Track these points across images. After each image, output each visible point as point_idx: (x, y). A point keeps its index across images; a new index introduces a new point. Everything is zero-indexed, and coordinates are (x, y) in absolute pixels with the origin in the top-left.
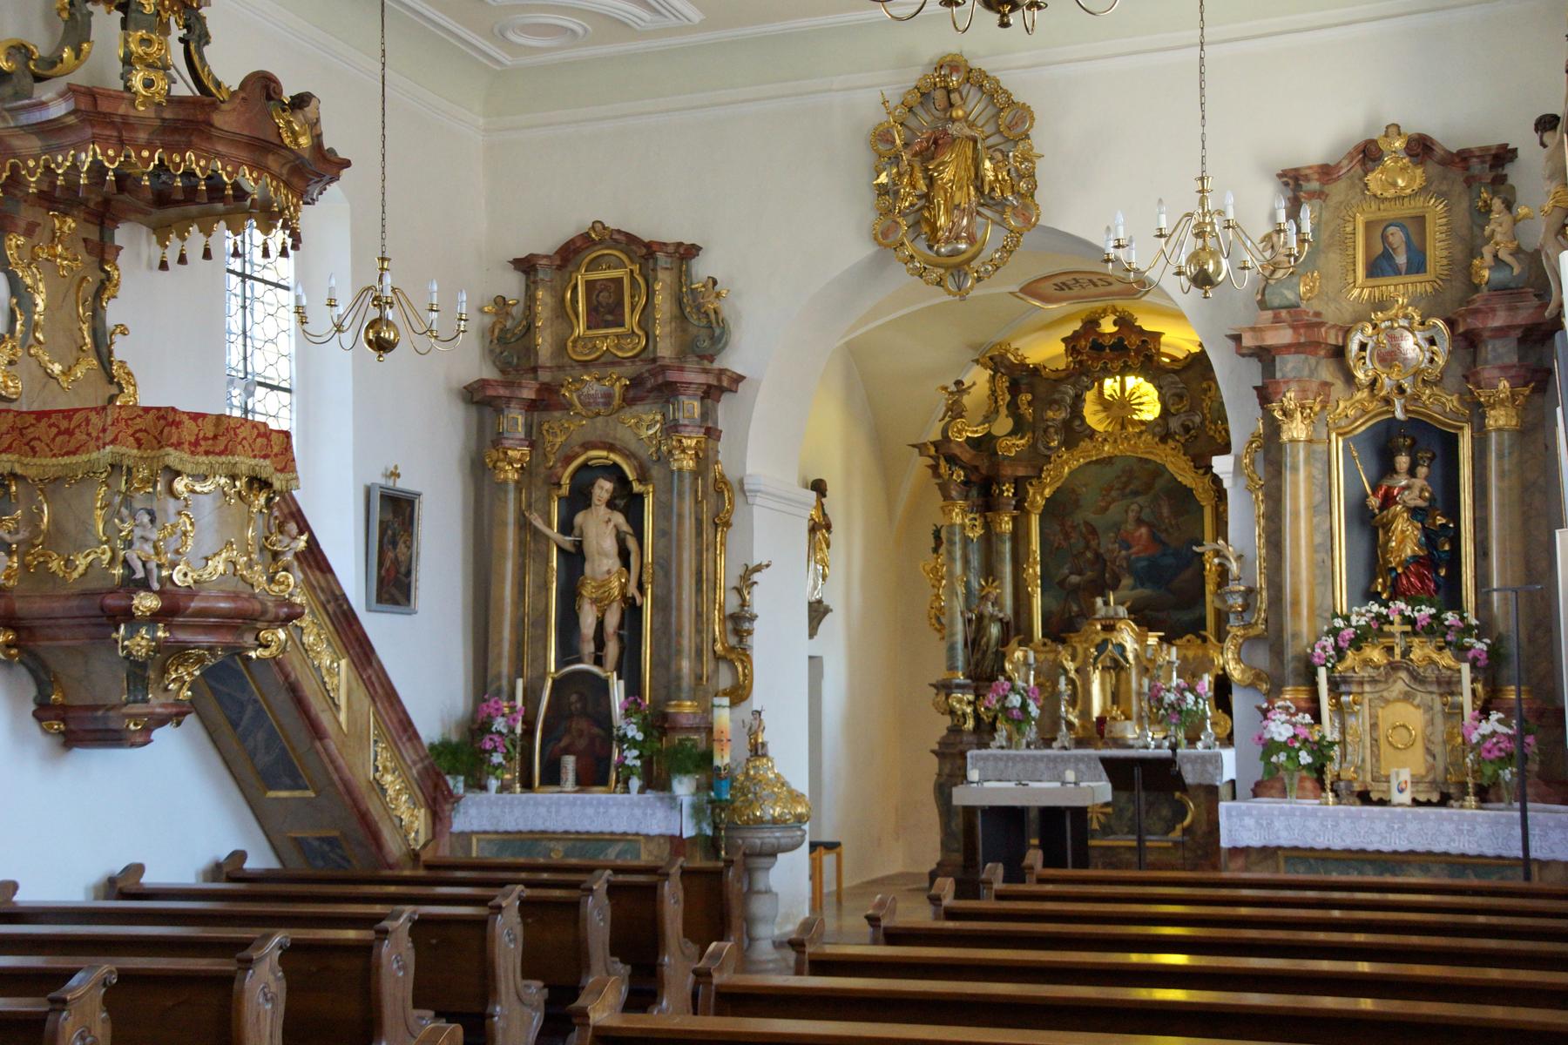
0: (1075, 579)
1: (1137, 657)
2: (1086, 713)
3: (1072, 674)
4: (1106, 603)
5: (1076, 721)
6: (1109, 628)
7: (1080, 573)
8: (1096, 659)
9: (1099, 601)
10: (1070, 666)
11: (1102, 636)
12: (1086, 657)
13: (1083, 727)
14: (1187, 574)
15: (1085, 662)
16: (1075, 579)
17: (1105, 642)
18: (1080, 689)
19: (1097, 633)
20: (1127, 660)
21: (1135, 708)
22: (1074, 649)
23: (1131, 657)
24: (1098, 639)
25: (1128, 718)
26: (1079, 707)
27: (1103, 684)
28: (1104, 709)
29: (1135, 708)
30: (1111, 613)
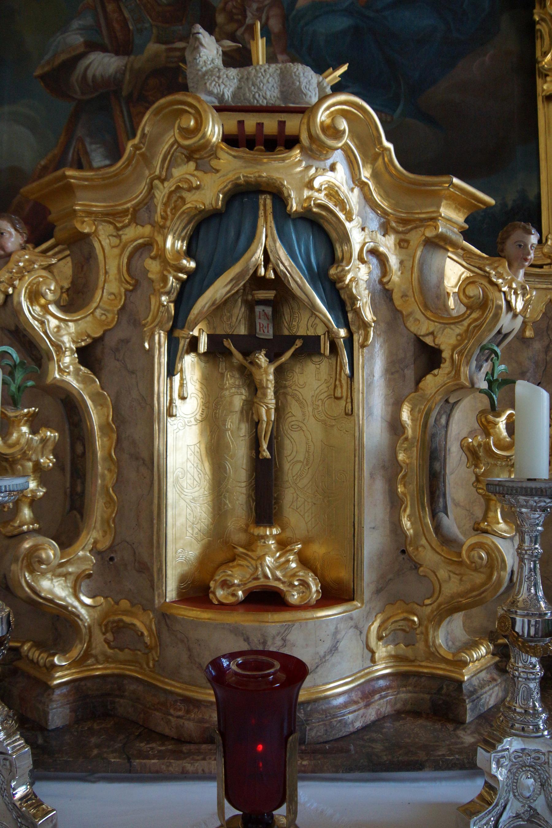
0: (103, 64)
1: (384, 293)
2: (130, 559)
3: (66, 370)
4: (238, 58)
5: (83, 606)
6: (270, 135)
7: (123, 48)
8: (185, 297)
9: (209, 50)
10: (60, 331)
11: (232, 167)
12: (137, 283)
13: (115, 628)
14: (476, 67)
15: (130, 314)
16: (103, 64)
17: (244, 197)
18: (100, 445)
19: (199, 154)
20: (340, 301)
21: (373, 542)
22: (80, 247)
23: (359, 276)
24: (210, 193)
25: (334, 594)
26: (93, 535)
27: (212, 421)
28: (221, 549)
29: (373, 542)
30: (269, 90)
